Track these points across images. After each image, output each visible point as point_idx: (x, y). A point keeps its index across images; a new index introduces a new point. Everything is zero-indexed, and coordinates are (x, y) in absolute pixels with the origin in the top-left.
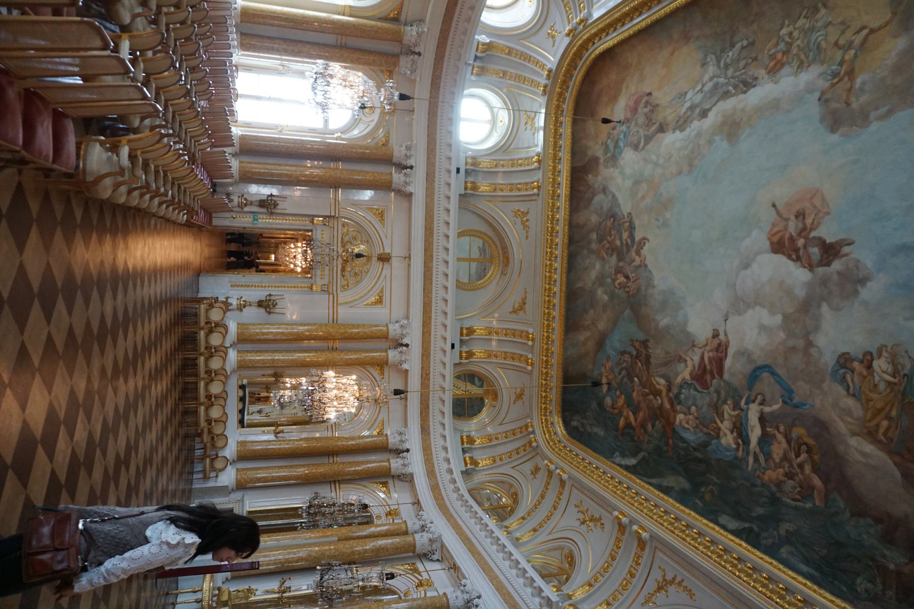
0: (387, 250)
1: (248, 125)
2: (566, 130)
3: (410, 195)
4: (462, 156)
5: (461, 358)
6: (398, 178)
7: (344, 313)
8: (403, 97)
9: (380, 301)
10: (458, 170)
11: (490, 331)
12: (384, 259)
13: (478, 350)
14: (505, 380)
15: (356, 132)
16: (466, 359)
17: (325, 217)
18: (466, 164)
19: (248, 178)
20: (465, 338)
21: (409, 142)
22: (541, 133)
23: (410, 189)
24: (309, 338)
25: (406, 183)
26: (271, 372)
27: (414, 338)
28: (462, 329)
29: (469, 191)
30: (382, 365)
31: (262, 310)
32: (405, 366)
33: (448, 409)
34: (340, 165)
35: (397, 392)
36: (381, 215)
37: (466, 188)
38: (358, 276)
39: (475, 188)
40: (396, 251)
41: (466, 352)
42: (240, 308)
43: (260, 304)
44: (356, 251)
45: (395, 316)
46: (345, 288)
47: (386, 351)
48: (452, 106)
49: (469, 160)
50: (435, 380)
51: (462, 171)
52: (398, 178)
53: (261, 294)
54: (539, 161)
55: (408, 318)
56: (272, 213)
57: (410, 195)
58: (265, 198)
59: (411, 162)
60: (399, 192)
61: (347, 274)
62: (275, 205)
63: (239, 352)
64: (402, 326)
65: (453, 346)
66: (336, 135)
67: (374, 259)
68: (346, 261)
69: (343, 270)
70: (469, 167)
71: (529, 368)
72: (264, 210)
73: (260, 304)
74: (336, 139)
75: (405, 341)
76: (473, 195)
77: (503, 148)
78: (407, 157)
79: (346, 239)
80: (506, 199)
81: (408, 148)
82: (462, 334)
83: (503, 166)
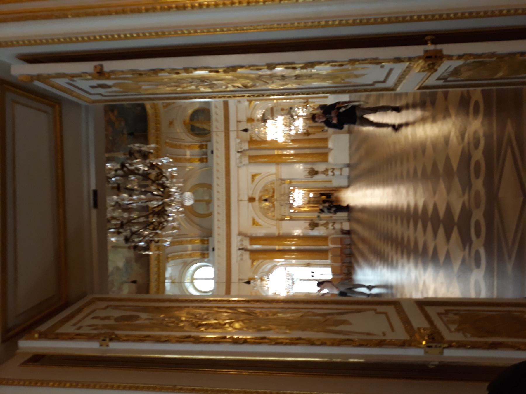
0: (250, 204)
1: (326, 266)
2: (153, 277)
3: (240, 234)
4: (211, 258)
5: (206, 145)
6: (246, 244)
7: (272, 169)
8: (248, 282)
9: (254, 176)
10: (213, 249)
11: (189, 161)
12: (252, 200)
13: (197, 150)
14: (180, 132)
15: (269, 266)
16: (203, 145)
17: (284, 220)
18: (208, 254)
19: (324, 239)
20: (204, 157)
21: (241, 263)
22: (167, 275)
23: (240, 238)
24: (291, 155)
25: (241, 240)
26: (311, 137)
27: (234, 156)
28: (207, 162)
29: (206, 238)
30: (251, 141)
31: (316, 169)
32: (238, 140)
33: (214, 117)
34: (277, 247)
35: (246, 130)
36: (254, 223)
37: (208, 240)
38: (265, 190)
39: (203, 241)
40: (245, 203)
41: (203, 148)
42: (327, 170)
43: (316, 173)
44: (267, 203)
45: (245, 168)
46: (272, 183)
47: (250, 149)
48: (217, 283)
49: (206, 256)
50: (222, 135)
51: (211, 249)
52: (246, 244)
53: (316, 177)
54: (168, 258)
55: (238, 167)
56: (311, 220)
57: (240, 234)
58: (316, 228)
59: (240, 252)
60: (245, 235)
61: (272, 190)
62: (310, 225)
63: (326, 147)
64: (241, 163)
65: (212, 152)
66: (279, 264)
67: (257, 198)
68: (273, 196)
69: (274, 192)
70: (206, 252)
71: (167, 141)
72: (316, 222)
73: (316, 173)
74: (279, 262)
75: (239, 155)
76: (204, 237)
77: (186, 265)
78: (242, 255)
79: (272, 209)
80: (186, 235)
81: (242, 259)
82: (207, 158)
83: (187, 255)
